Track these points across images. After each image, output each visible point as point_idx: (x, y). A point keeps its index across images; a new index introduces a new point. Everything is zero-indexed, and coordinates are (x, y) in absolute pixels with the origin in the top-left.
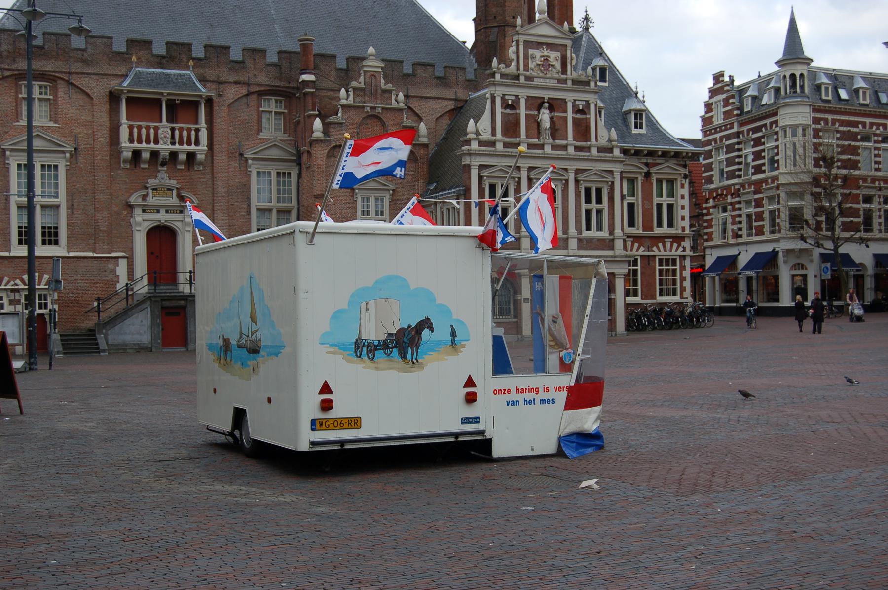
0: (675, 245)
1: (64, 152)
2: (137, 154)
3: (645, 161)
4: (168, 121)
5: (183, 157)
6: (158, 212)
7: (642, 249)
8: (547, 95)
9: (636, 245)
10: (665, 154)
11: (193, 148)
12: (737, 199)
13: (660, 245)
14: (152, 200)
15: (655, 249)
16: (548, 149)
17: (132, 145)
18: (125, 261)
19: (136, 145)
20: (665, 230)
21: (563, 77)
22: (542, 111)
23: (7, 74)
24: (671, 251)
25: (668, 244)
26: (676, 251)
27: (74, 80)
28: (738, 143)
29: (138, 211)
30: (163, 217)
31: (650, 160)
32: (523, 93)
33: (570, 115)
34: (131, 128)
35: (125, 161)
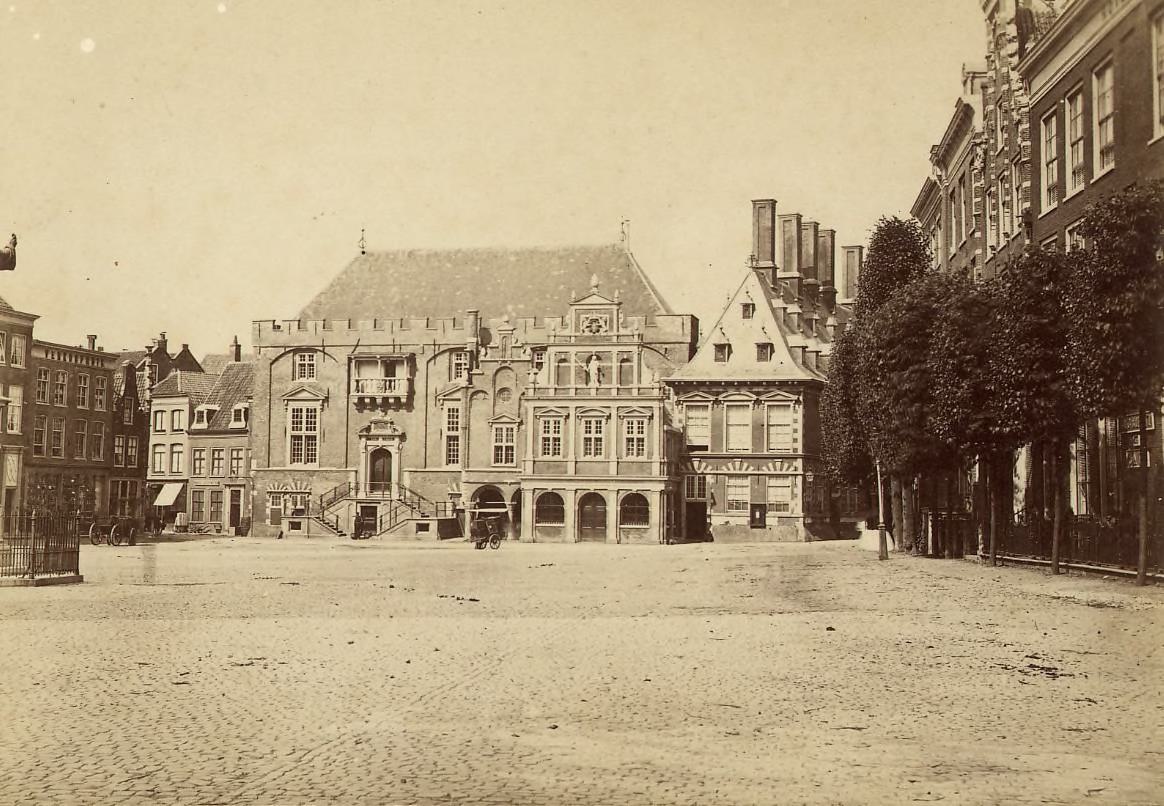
0: (786, 465)
2: (361, 399)
5: (391, 401)
6: (378, 439)
7: (752, 468)
8: (594, 349)
9: (745, 465)
13: (770, 465)
14: (371, 433)
15: (764, 468)
16: (593, 392)
19: (360, 394)
21: (610, 334)
23: (287, 349)
24: (781, 470)
25: (778, 464)
29: (364, 439)
30: (380, 443)
31: (761, 390)
32: (573, 350)
33: (615, 365)
34: (357, 381)
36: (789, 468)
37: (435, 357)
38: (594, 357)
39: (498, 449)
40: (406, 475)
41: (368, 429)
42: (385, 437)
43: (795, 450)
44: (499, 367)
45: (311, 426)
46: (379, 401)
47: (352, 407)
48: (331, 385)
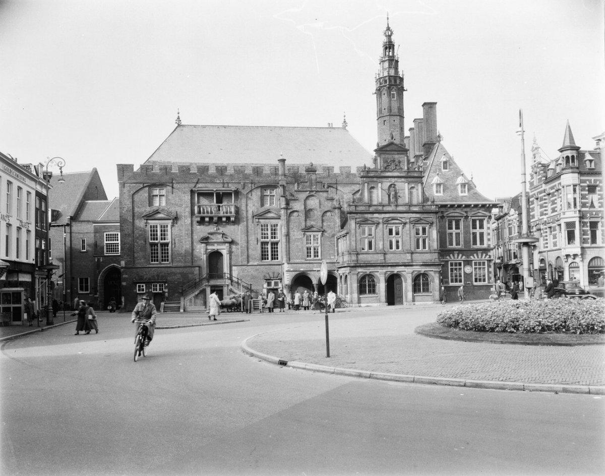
0: (484, 255)
1: (170, 219)
2: (203, 219)
3: (465, 210)
4: (217, 203)
7: (464, 257)
9: (460, 255)
10: (476, 206)
11: (229, 215)
12: (545, 227)
13: (475, 255)
17: (200, 215)
18: (198, 268)
19: (202, 215)
20: (478, 246)
22: (391, 189)
23: (145, 185)
26: (485, 257)
27: (175, 185)
28: (545, 196)
30: (215, 247)
35: (198, 222)
36: (486, 256)
37: (251, 191)
38: (393, 186)
39: (309, 249)
40: (234, 268)
41: (207, 238)
42: (219, 243)
43: (489, 245)
44: (308, 195)
45: (164, 236)
46: (215, 219)
47: (195, 223)
48: (179, 210)
